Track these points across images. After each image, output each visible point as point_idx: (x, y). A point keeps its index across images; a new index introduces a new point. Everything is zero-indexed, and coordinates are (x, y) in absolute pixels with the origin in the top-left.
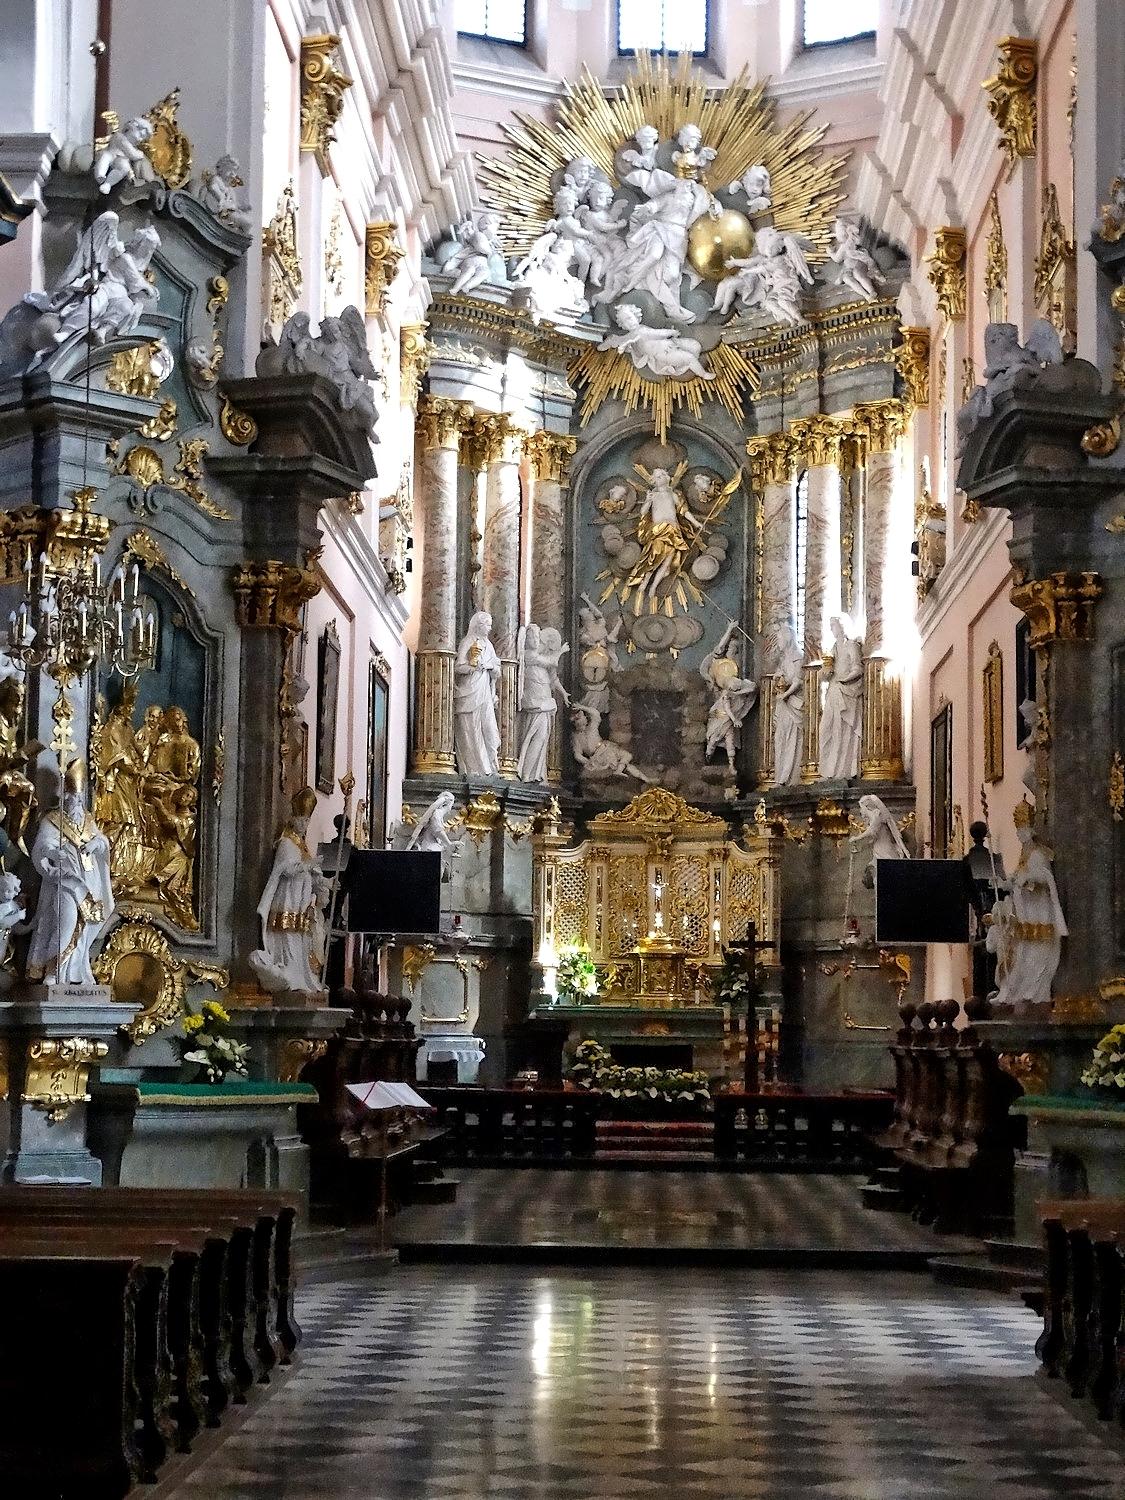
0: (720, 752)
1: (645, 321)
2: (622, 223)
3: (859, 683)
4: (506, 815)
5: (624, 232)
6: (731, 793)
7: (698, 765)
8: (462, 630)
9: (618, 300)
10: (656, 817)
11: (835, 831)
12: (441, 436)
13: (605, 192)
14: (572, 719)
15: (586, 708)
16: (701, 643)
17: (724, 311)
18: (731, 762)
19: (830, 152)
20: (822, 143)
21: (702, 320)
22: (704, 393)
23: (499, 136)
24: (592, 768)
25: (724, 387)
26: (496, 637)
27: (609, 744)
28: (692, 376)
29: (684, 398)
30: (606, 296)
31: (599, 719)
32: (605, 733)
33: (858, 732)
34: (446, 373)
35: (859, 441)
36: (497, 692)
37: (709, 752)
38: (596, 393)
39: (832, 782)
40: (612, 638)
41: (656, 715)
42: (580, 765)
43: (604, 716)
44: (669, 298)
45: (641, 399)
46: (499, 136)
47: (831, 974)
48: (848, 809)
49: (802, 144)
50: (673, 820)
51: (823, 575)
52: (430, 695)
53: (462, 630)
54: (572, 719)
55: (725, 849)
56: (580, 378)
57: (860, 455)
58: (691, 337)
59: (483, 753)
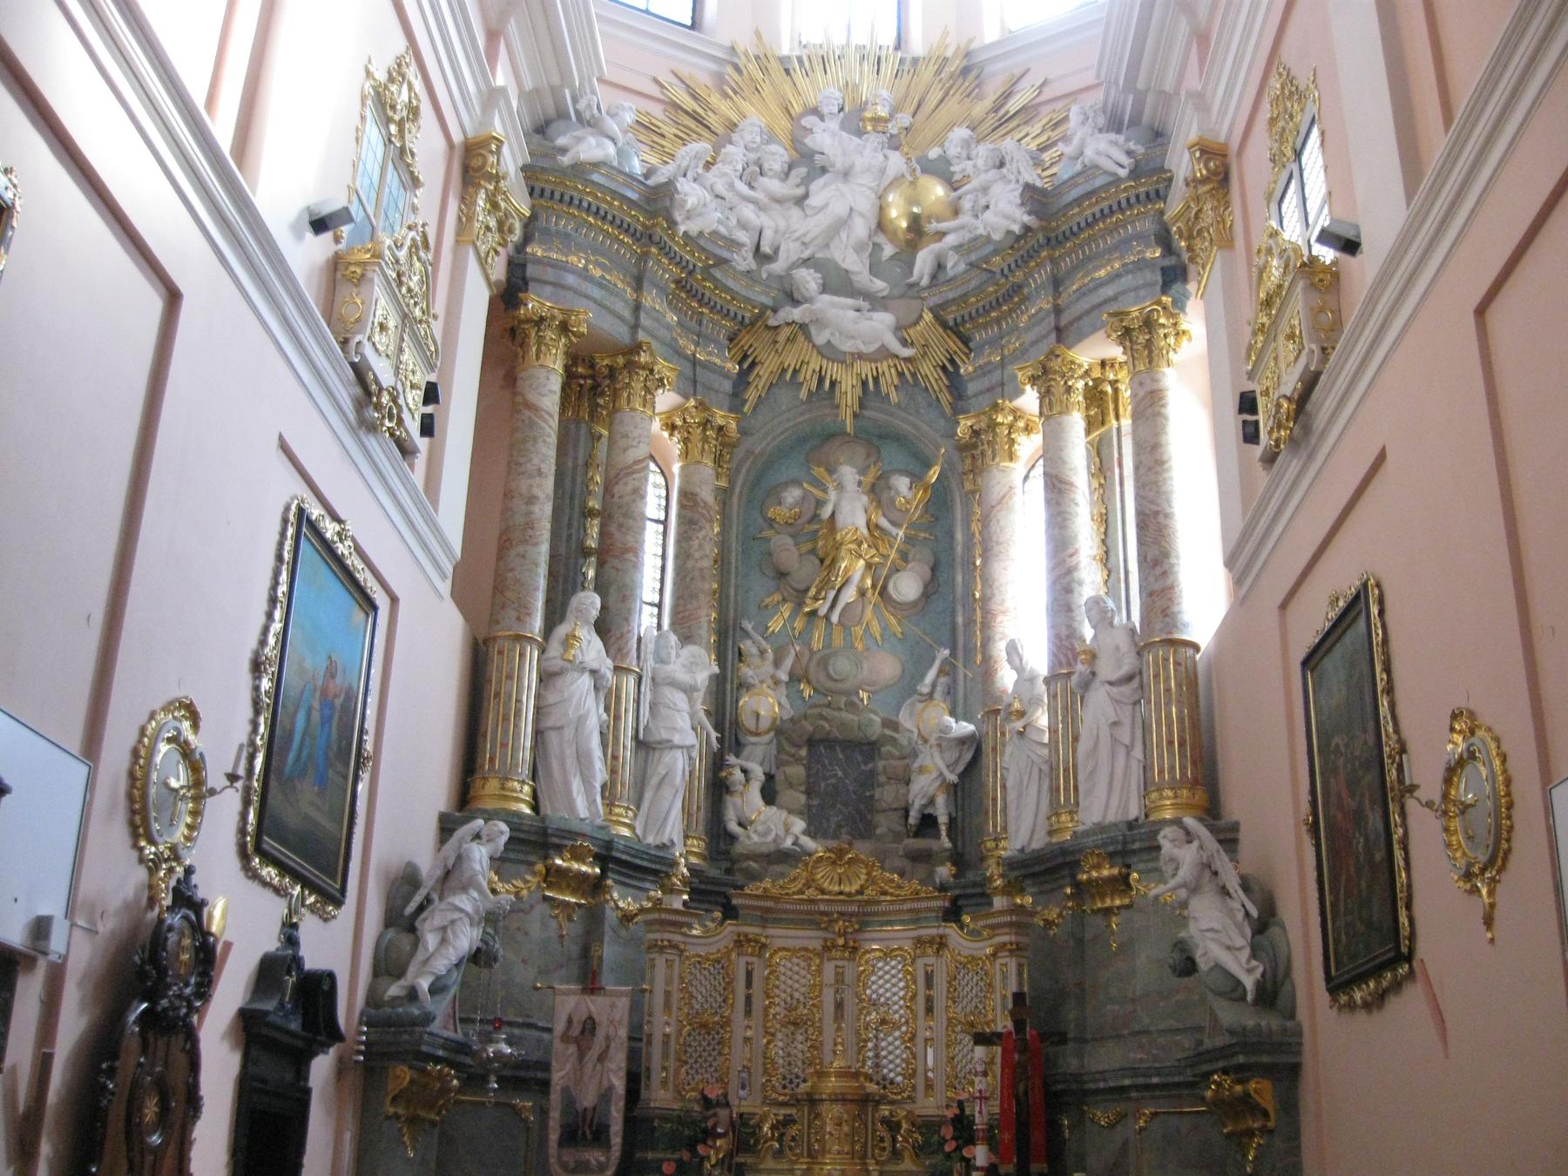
0: (928, 823)
1: (825, 289)
2: (800, 191)
3: (1135, 683)
4: (609, 882)
5: (800, 201)
6: (944, 872)
7: (897, 837)
8: (555, 613)
9: (795, 265)
10: (836, 888)
11: (1108, 903)
12: (539, 351)
13: (777, 156)
14: (724, 774)
15: (743, 763)
16: (907, 687)
17: (925, 282)
18: (944, 833)
19: (1045, 110)
20: (1038, 100)
21: (896, 292)
22: (901, 375)
23: (654, 91)
24: (751, 840)
25: (927, 369)
26: (603, 628)
27: (773, 810)
28: (884, 353)
29: (876, 379)
30: (778, 267)
31: (763, 778)
32: (769, 795)
33: (1138, 752)
34: (550, 274)
35: (1109, 389)
36: (607, 709)
37: (912, 821)
38: (764, 373)
39: (1100, 828)
40: (784, 677)
41: (840, 774)
42: (732, 838)
43: (769, 777)
44: (855, 264)
45: (821, 380)
46: (654, 91)
47: (1111, 1126)
48: (1128, 866)
49: (1013, 105)
50: (860, 892)
51: (1070, 551)
52: (497, 695)
53: (555, 613)
54: (724, 774)
55: (941, 937)
56: (745, 357)
57: (1111, 406)
58: (886, 309)
59: (576, 785)
